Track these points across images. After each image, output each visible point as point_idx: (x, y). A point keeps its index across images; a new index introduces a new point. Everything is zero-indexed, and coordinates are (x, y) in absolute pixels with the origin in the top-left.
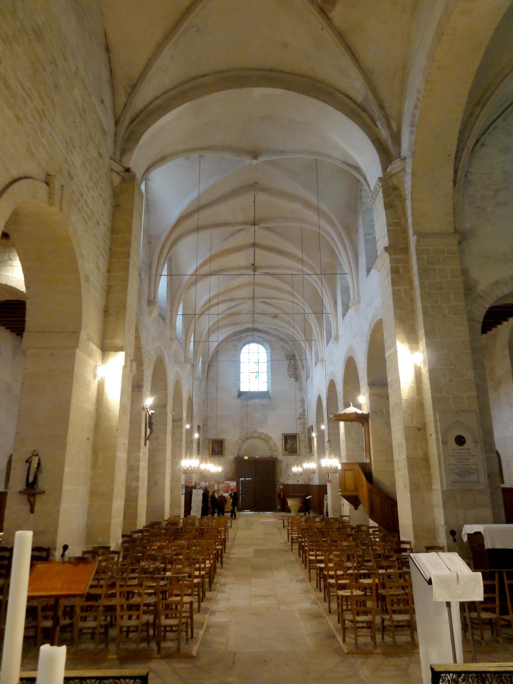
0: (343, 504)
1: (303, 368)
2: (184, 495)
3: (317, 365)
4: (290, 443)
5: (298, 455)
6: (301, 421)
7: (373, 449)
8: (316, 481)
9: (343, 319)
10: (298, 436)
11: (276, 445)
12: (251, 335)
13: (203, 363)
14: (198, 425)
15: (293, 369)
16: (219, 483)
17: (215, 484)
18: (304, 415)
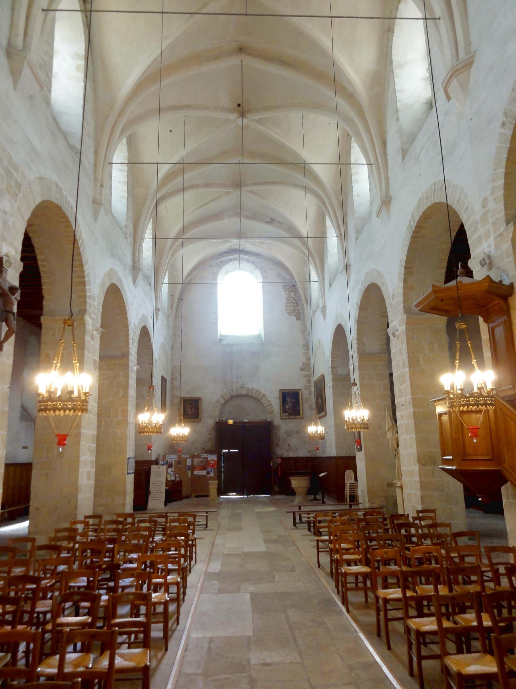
0: (401, 487)
1: (307, 302)
3: (333, 285)
4: (290, 402)
5: (302, 418)
6: (305, 373)
9: (403, 160)
10: (300, 393)
11: (271, 404)
12: (235, 259)
13: (171, 295)
14: (163, 377)
15: (294, 303)
16: (193, 457)
17: (187, 458)
18: (309, 364)
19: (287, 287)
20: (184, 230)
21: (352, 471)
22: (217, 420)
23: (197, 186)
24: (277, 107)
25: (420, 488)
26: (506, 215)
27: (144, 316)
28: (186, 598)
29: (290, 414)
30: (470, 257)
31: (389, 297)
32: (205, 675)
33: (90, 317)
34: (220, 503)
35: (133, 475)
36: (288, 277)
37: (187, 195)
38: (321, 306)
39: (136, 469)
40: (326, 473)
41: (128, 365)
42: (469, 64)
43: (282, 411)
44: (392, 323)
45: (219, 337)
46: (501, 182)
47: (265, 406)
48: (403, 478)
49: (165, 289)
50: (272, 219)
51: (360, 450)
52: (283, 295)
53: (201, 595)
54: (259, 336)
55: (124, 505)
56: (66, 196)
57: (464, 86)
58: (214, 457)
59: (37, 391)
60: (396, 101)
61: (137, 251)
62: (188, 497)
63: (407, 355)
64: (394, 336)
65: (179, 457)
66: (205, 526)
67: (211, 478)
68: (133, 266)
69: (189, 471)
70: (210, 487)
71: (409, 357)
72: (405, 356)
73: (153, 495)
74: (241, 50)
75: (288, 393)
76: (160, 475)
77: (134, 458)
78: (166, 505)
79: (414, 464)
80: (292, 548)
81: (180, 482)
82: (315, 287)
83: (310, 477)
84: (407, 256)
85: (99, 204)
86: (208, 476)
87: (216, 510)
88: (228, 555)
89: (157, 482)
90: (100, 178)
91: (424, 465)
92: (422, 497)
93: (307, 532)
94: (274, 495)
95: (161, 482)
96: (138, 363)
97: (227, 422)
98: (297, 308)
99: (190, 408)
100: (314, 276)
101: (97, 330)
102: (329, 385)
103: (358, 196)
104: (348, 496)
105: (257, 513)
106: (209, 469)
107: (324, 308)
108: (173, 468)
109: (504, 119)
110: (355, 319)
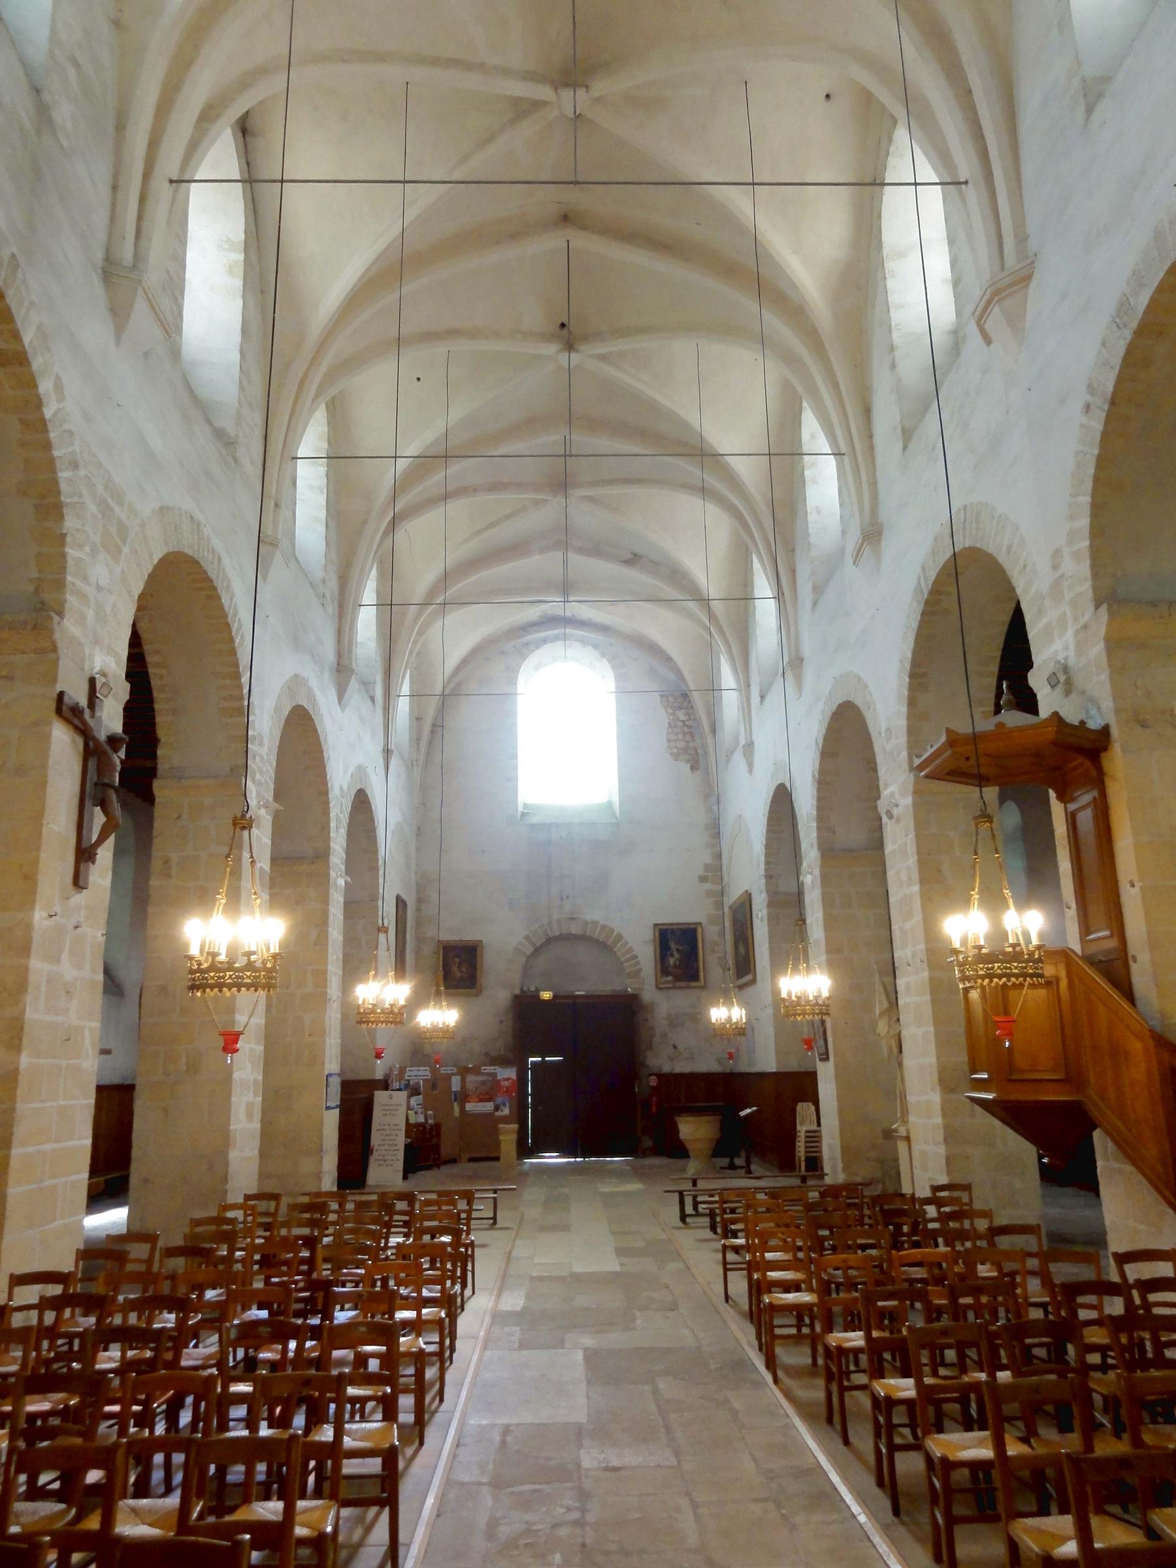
0: (908, 1139)
1: (714, 731)
2: (336, 1113)
3: (768, 698)
4: (678, 950)
5: (703, 988)
6: (708, 886)
7: (1138, 885)
8: (766, 1060)
9: (905, 448)
11: (636, 957)
12: (556, 638)
13: (417, 718)
15: (684, 734)
16: (464, 1072)
19: (670, 698)
20: (447, 578)
21: (810, 1104)
22: (517, 992)
23: (474, 490)
24: (642, 330)
25: (945, 1140)
26: (1095, 588)
27: (361, 771)
28: (455, 1356)
29: (677, 978)
30: (1031, 666)
31: (880, 734)
32: (497, 1484)
33: (253, 780)
34: (524, 1175)
35: (337, 1111)
36: (672, 676)
37: (455, 507)
38: (743, 742)
39: (342, 1100)
40: (754, 1108)
41: (328, 875)
42: (1024, 279)
43: (659, 973)
44: (886, 789)
45: (520, 808)
46: (1084, 522)
47: (622, 959)
48: (912, 1118)
49: (403, 706)
50: (635, 555)
51: (825, 1057)
52: (661, 717)
53: (488, 1353)
54: (609, 804)
55: (319, 1177)
56: (209, 539)
57: (1015, 321)
58: (511, 1073)
59: (188, 951)
60: (891, 327)
61: (347, 636)
62: (453, 1161)
63: (916, 857)
64: (890, 817)
65: (434, 1072)
66: (492, 1221)
67: (505, 1120)
68: (338, 664)
69: (456, 1104)
70: (501, 1137)
71: (920, 861)
72: (912, 861)
73: (379, 1155)
74: (566, 218)
75: (673, 932)
76: (393, 1112)
77: (339, 1075)
78: (405, 1177)
79: (932, 1090)
80: (672, 1266)
81: (437, 1127)
82: (730, 701)
83: (720, 1118)
84: (915, 652)
85: (271, 544)
86: (497, 1114)
87: (515, 1187)
88: (541, 1279)
89: (387, 1127)
90: (274, 492)
91: (952, 1091)
92: (948, 1158)
93: (708, 1234)
94: (642, 1157)
95: (396, 1127)
96: (348, 872)
97: (538, 997)
98: (691, 745)
99: (457, 965)
100: (727, 677)
101: (266, 807)
102: (760, 914)
103: (818, 512)
104: (803, 1158)
105: (603, 1195)
106: (499, 1100)
107: (749, 748)
108: (421, 1096)
109: (1089, 398)
110: (813, 776)
